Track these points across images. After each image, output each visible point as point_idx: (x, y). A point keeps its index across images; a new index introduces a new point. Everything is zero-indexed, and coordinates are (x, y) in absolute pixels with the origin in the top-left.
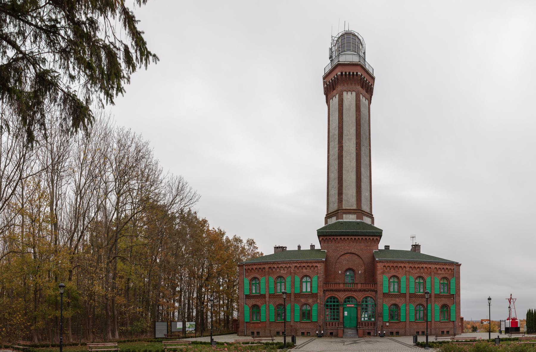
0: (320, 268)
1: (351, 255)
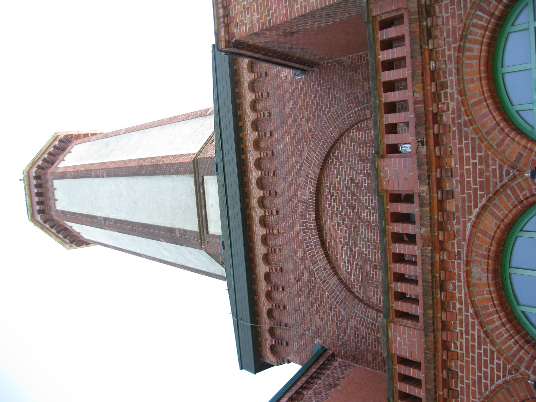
1: (328, 205)
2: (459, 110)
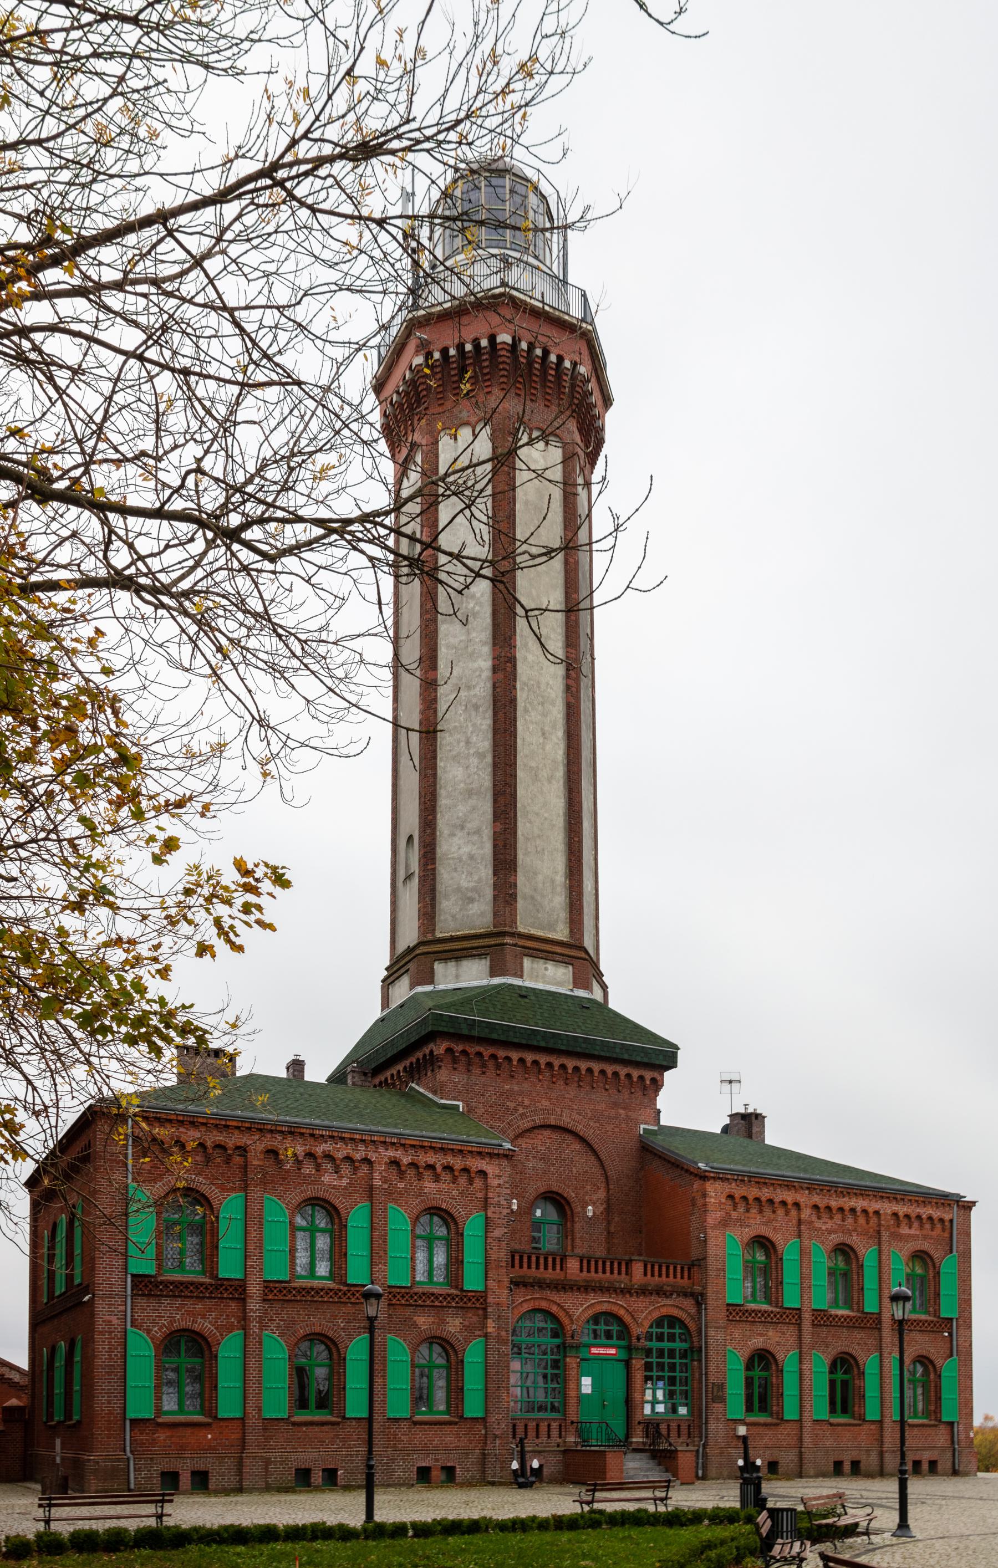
0: (496, 1182)
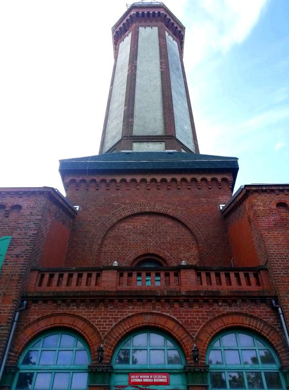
1: (153, 219)
2: (220, 312)
